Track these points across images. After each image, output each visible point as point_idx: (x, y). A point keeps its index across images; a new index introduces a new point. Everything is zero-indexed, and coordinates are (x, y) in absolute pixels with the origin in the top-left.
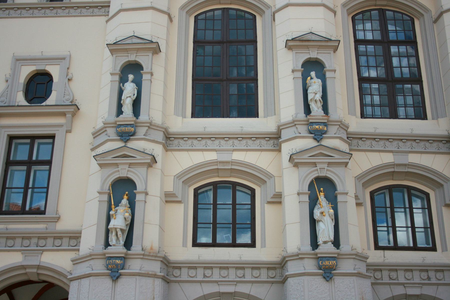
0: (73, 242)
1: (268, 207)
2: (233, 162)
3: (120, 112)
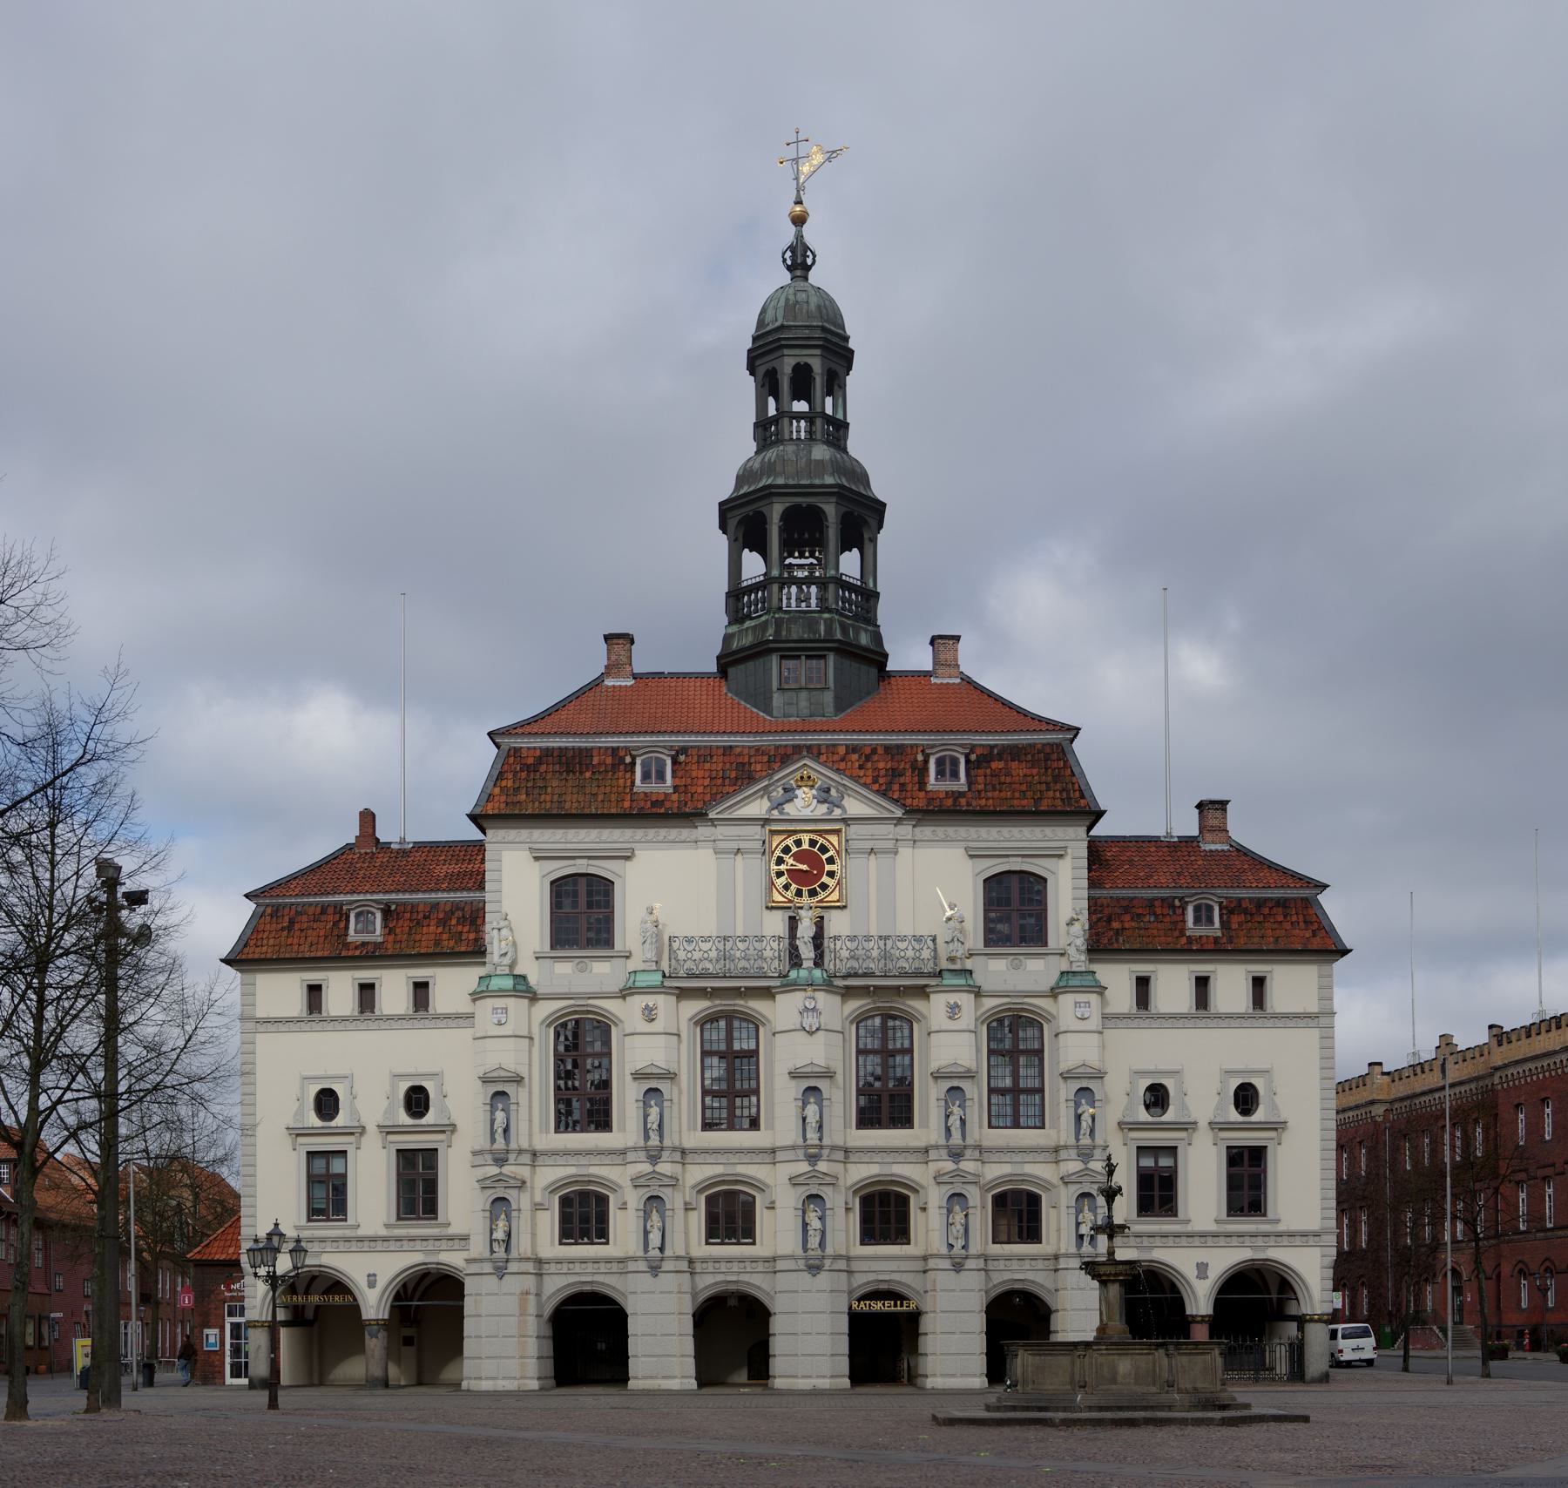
0: (463, 1242)
1: (618, 1212)
2: (589, 1176)
3: (493, 1140)
